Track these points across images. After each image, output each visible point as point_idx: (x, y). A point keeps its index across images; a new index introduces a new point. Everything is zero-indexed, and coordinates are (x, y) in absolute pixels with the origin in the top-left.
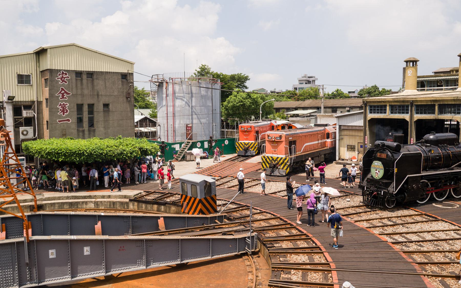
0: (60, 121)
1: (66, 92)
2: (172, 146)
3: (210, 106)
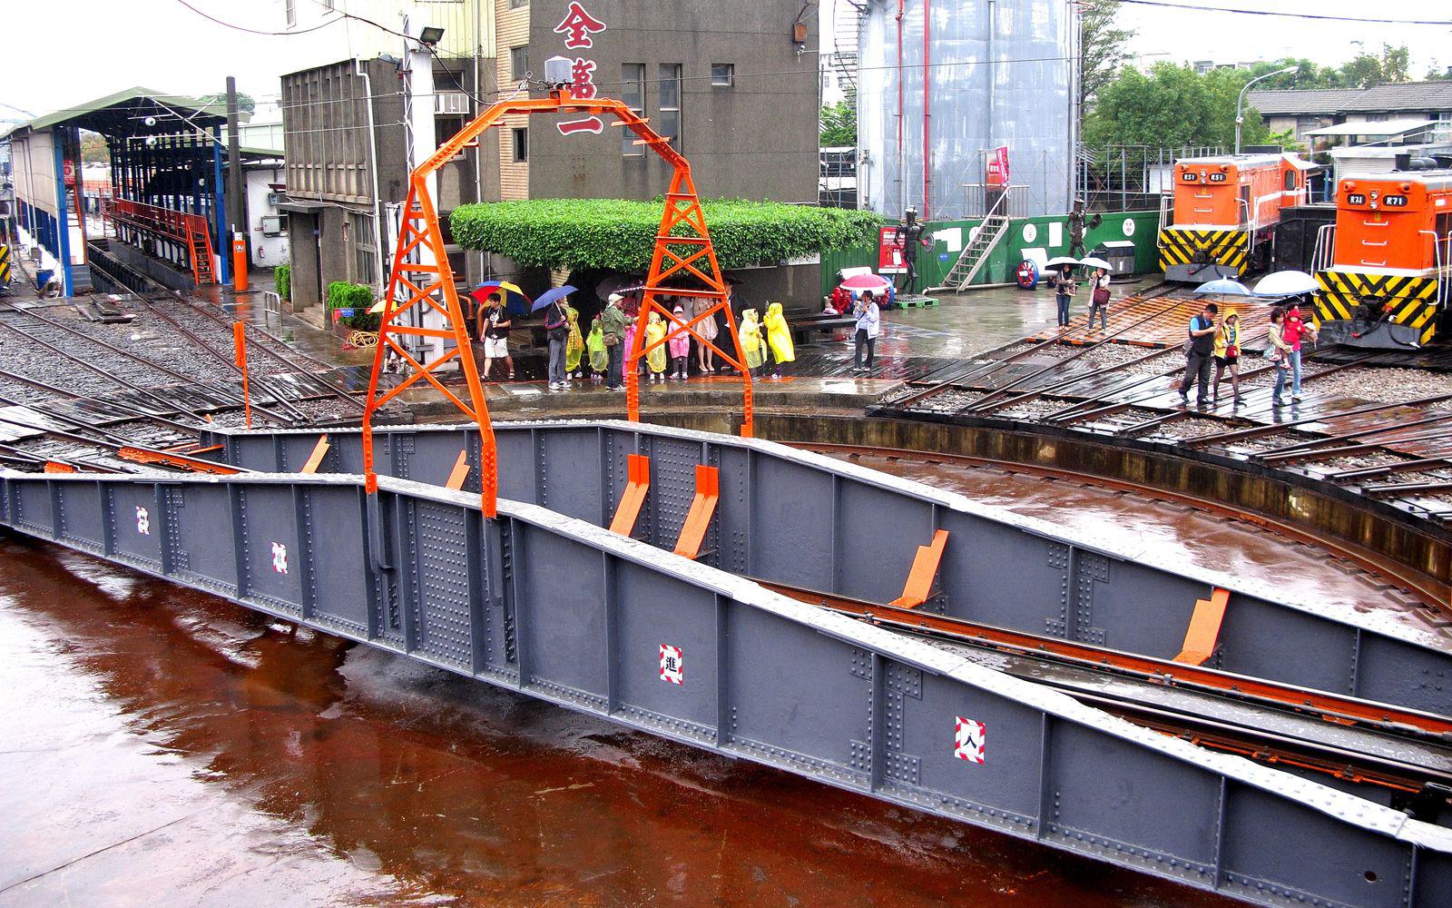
0: (565, 128)
1: (586, 21)
2: (937, 235)
3: (1061, 88)
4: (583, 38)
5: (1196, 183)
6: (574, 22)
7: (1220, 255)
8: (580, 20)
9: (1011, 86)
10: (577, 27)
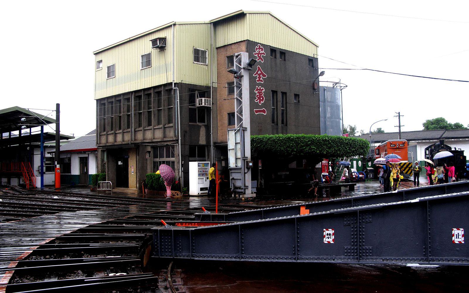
0: (257, 112)
1: (262, 73)
4: (261, 79)
5: (395, 147)
6: (259, 73)
7: (404, 170)
8: (260, 73)
9: (331, 118)
10: (259, 75)
